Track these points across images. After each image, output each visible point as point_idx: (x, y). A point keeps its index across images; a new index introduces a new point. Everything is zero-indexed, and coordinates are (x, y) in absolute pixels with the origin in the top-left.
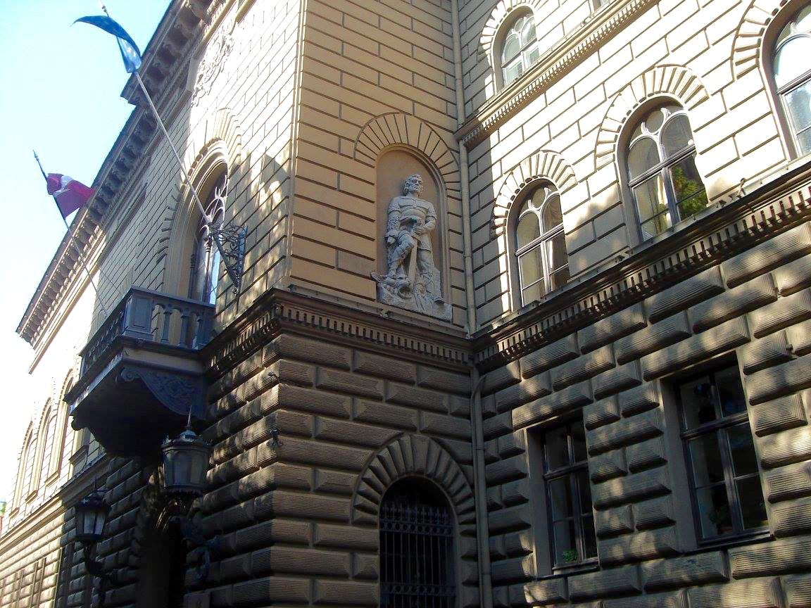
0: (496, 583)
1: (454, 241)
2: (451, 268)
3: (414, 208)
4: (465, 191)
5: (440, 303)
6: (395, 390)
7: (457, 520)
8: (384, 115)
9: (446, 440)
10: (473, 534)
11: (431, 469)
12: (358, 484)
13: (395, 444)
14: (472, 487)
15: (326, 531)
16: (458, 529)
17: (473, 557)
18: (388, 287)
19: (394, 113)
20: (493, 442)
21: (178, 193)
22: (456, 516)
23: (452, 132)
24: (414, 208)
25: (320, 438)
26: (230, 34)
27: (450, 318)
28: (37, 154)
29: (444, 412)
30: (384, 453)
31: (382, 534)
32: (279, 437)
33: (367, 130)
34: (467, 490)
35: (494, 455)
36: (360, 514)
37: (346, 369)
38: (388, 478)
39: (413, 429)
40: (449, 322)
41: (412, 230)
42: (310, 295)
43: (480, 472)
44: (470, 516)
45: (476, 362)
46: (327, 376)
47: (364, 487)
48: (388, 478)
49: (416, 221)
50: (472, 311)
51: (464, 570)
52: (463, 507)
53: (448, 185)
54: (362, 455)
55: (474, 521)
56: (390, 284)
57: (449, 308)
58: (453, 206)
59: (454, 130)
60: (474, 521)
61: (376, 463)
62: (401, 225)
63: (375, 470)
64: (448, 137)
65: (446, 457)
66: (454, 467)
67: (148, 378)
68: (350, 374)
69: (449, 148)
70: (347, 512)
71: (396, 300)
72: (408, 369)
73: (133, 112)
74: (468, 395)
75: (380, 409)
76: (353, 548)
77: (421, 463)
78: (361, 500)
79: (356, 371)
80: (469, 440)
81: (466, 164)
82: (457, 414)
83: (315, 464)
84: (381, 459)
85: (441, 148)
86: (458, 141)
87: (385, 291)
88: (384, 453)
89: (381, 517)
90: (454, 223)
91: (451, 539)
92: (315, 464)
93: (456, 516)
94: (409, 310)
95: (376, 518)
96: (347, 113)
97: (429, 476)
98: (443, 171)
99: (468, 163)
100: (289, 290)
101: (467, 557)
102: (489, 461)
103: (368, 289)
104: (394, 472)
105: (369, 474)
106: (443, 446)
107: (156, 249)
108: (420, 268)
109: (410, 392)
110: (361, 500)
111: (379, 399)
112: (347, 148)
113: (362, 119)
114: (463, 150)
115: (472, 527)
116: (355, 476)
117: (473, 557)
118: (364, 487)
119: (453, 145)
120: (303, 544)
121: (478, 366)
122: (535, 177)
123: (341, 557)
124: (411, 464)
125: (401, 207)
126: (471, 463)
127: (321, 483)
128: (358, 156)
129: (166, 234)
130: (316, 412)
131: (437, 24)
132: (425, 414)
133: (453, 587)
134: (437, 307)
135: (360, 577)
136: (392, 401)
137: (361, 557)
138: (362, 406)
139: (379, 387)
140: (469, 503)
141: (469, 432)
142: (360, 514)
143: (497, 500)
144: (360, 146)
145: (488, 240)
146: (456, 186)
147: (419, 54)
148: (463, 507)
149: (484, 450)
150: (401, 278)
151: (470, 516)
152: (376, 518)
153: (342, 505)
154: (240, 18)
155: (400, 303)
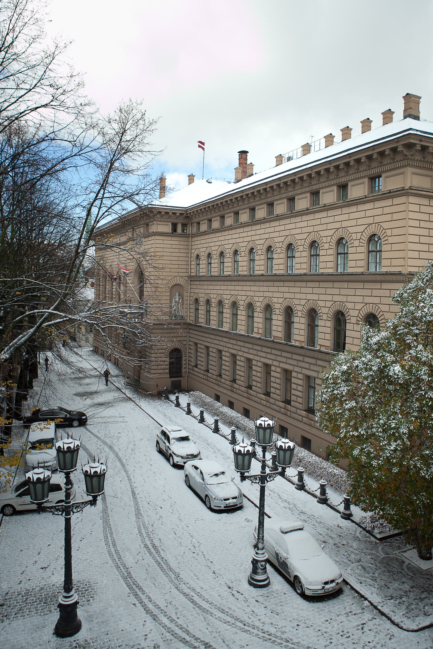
7: (183, 354)
16: (183, 356)
33: (168, 284)
36: (166, 356)
47: (166, 352)
51: (184, 362)
61: (168, 348)
64: (186, 278)
76: (164, 361)
77: (176, 347)
78: (166, 354)
85: (185, 281)
101: (185, 360)
103: (168, 318)
105: (167, 350)
110: (166, 354)
118: (166, 352)
128: (166, 291)
142: (166, 356)
147: (181, 259)
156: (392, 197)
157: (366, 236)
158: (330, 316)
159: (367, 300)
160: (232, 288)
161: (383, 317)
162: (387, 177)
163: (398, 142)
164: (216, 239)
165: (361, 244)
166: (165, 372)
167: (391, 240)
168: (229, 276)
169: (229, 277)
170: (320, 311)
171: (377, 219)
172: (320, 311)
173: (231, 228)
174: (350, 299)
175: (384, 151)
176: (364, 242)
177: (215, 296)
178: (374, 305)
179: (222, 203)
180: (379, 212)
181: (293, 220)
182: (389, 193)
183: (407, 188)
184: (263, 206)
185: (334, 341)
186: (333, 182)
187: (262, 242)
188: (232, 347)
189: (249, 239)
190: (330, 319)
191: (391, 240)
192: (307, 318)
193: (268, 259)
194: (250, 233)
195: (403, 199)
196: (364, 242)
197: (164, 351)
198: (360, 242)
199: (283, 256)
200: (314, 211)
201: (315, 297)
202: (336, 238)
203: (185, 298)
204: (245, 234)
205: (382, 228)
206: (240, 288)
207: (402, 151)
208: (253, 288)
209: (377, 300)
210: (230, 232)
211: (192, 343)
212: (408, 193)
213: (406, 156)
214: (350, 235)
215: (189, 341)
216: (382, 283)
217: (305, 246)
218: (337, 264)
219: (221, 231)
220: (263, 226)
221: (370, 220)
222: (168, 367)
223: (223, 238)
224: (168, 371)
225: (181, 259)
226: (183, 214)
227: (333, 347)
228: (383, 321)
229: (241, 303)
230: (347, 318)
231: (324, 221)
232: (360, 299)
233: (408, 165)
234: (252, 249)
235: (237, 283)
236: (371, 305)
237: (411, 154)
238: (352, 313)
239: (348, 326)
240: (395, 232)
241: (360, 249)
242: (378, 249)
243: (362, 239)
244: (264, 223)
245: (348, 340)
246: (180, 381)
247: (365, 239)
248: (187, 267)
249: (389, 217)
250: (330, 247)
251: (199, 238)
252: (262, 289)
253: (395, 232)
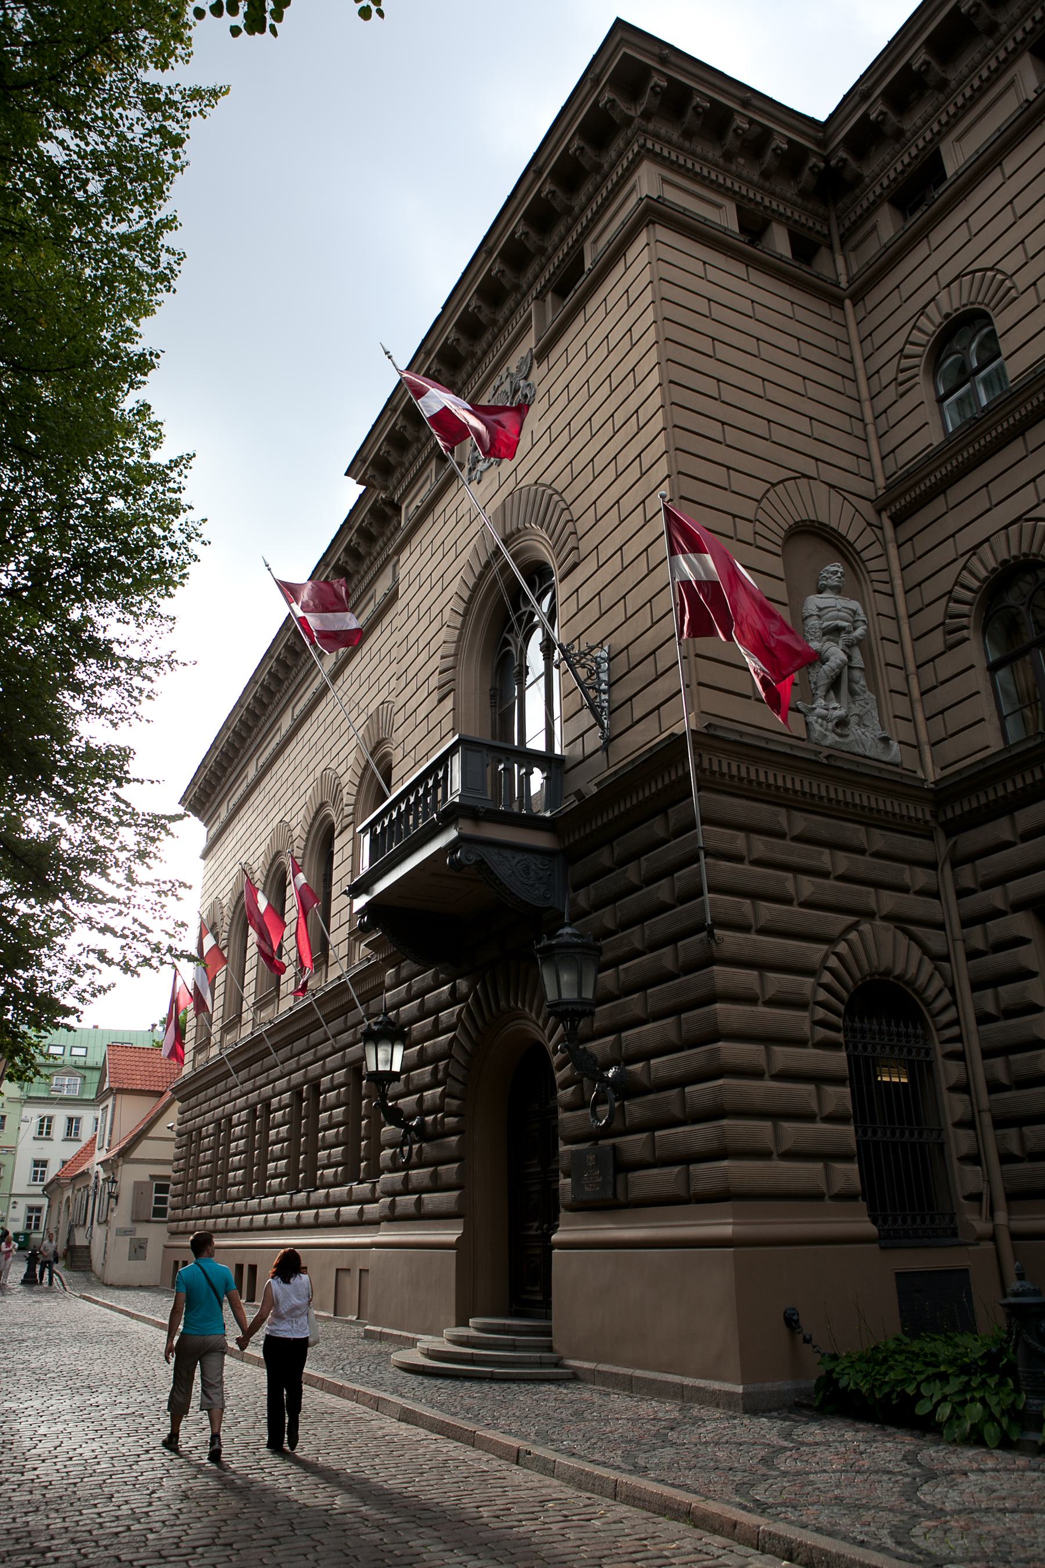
0: (999, 1124)
1: (892, 653)
2: (891, 691)
3: (839, 610)
4: (898, 582)
5: (885, 740)
6: (844, 862)
8: (782, 482)
9: (913, 928)
10: (960, 1056)
11: (898, 971)
12: (814, 993)
13: (853, 936)
14: (952, 991)
15: (785, 1056)
16: (939, 1050)
17: (963, 1088)
18: (820, 720)
19: (794, 478)
20: (978, 929)
21: (464, 605)
22: (934, 1033)
23: (872, 501)
24: (839, 610)
25: (763, 931)
26: (526, 378)
27: (898, 760)
28: (268, 562)
29: (905, 890)
30: (842, 948)
31: (849, 1056)
32: (716, 931)
34: (946, 997)
35: (981, 945)
36: (822, 1033)
37: (781, 835)
38: (850, 983)
39: (869, 915)
40: (896, 765)
41: (840, 642)
42: (733, 737)
43: (962, 971)
44: (954, 1031)
45: (942, 819)
46: (760, 846)
47: (823, 995)
48: (850, 983)
49: (843, 628)
50: (926, 749)
51: (955, 1106)
52: (945, 1018)
53: (874, 576)
54: (815, 952)
55: (958, 1039)
56: (823, 717)
57: (895, 746)
58: (884, 604)
59: (873, 497)
60: (958, 1039)
61: (833, 962)
62: (824, 635)
63: (831, 970)
64: (866, 508)
65: (916, 952)
66: (928, 966)
67: (492, 857)
68: (788, 842)
69: (870, 524)
70: (806, 1028)
71: (832, 738)
72: (855, 833)
73: (361, 496)
74: (933, 866)
75: (830, 889)
76: (820, 1079)
78: (821, 1013)
79: (795, 839)
80: (941, 926)
81: (894, 544)
82: (920, 893)
83: (762, 966)
84: (837, 954)
86: (879, 512)
87: (817, 727)
88: (842, 948)
89: (845, 1036)
90: (888, 628)
91: (930, 1065)
92: (762, 966)
93: (934, 1033)
94: (848, 752)
95: (840, 1037)
96: (739, 482)
97: (899, 977)
98: (865, 555)
99: (897, 542)
100: (705, 731)
102: (972, 955)
104: (858, 975)
105: (827, 978)
106: (912, 937)
107: (434, 682)
108: (852, 693)
109: (863, 865)
110: (821, 1013)
111: (825, 875)
112: (745, 530)
113: (757, 489)
114: (887, 524)
115: (958, 1046)
116: (811, 980)
117: (963, 1088)
118: (823, 995)
119: (873, 519)
120: (756, 1074)
121: (942, 825)
122: (1034, 555)
124: (875, 962)
125: (820, 609)
126: (947, 958)
127: (771, 992)
129: (449, 662)
130: (755, 896)
131: (830, 345)
132: (884, 893)
133: (940, 1131)
134: (881, 745)
135: (830, 1119)
136: (842, 878)
137: (830, 1090)
138: (808, 886)
139: (825, 858)
140: (950, 1015)
141: (939, 917)
142: (822, 1033)
143: (990, 1008)
144: (759, 527)
145: (942, 650)
146: (884, 576)
147: (813, 390)
148: (945, 1018)
149: (964, 941)
150: (835, 708)
151: (954, 1031)
153: (798, 1021)
154: (542, 354)
155: (837, 742)
211: (1021, 924)
224: (848, 1174)
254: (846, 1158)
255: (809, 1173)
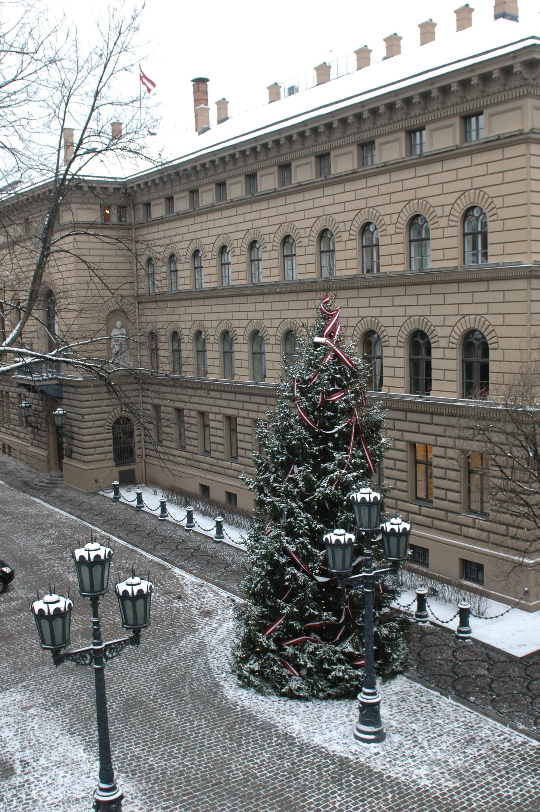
7: (135, 426)
13: (115, 411)
16: (135, 428)
30: (113, 413)
36: (106, 431)
46: (95, 397)
47: (107, 424)
51: (137, 439)
61: (110, 417)
78: (106, 427)
91: (133, 431)
105: (109, 420)
110: (106, 427)
114: (137, 304)
118: (107, 424)
120: (93, 441)
123: (102, 443)
137: (107, 441)
142: (106, 431)
147: (120, 266)
152: (111, 431)
156: (503, 146)
157: (459, 210)
158: (403, 340)
159: (465, 309)
160: (221, 308)
161: (493, 334)
162: (492, 115)
163: (514, 57)
164: (185, 230)
165: (451, 223)
166: (108, 458)
167: (502, 214)
168: (215, 289)
169: (214, 291)
170: (385, 333)
171: (477, 183)
172: (385, 333)
173: (211, 209)
174: (436, 310)
175: (490, 73)
176: (456, 219)
177: (189, 324)
178: (478, 317)
179: (195, 168)
180: (481, 170)
181: (328, 191)
182: (496, 140)
183: (526, 130)
184: (271, 170)
185: (411, 378)
186: (399, 125)
187: (274, 229)
188: (227, 405)
189: (248, 226)
190: (402, 345)
191: (502, 214)
192: (361, 346)
193: (284, 256)
194: (248, 217)
195: (521, 149)
196: (456, 219)
197: (103, 422)
198: (449, 220)
199: (313, 249)
200: (368, 174)
201: (375, 312)
202: (407, 215)
203: (131, 331)
204: (240, 219)
205: (486, 196)
206: (236, 308)
207: (521, 73)
208: (259, 307)
209: (482, 309)
210: (211, 216)
211: (149, 407)
212: (529, 138)
213: (526, 79)
214: (432, 209)
215: (143, 402)
216: (490, 282)
217: (352, 232)
218: (410, 258)
219: (194, 216)
220: (272, 203)
221: (466, 185)
222: (111, 448)
223: (198, 227)
224: (111, 455)
225: (120, 266)
226: (118, 189)
227: (409, 389)
228: (495, 339)
229: (240, 332)
230: (431, 341)
231: (384, 189)
232: (453, 309)
233: (529, 95)
234: (254, 242)
235: (229, 300)
236: (471, 317)
237: (534, 76)
238: (440, 331)
239: (435, 353)
240: (509, 201)
241: (449, 232)
242: (424, 236)
243: (452, 215)
244: (274, 198)
245: (435, 374)
246: (133, 471)
247: (457, 214)
248: (131, 279)
249: (497, 178)
250: (398, 230)
251: (151, 230)
252: (276, 306)
253: (509, 201)
254: (111, 452)
255: (102, 456)
